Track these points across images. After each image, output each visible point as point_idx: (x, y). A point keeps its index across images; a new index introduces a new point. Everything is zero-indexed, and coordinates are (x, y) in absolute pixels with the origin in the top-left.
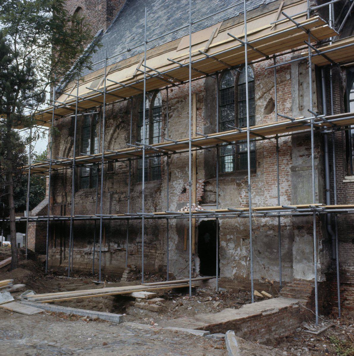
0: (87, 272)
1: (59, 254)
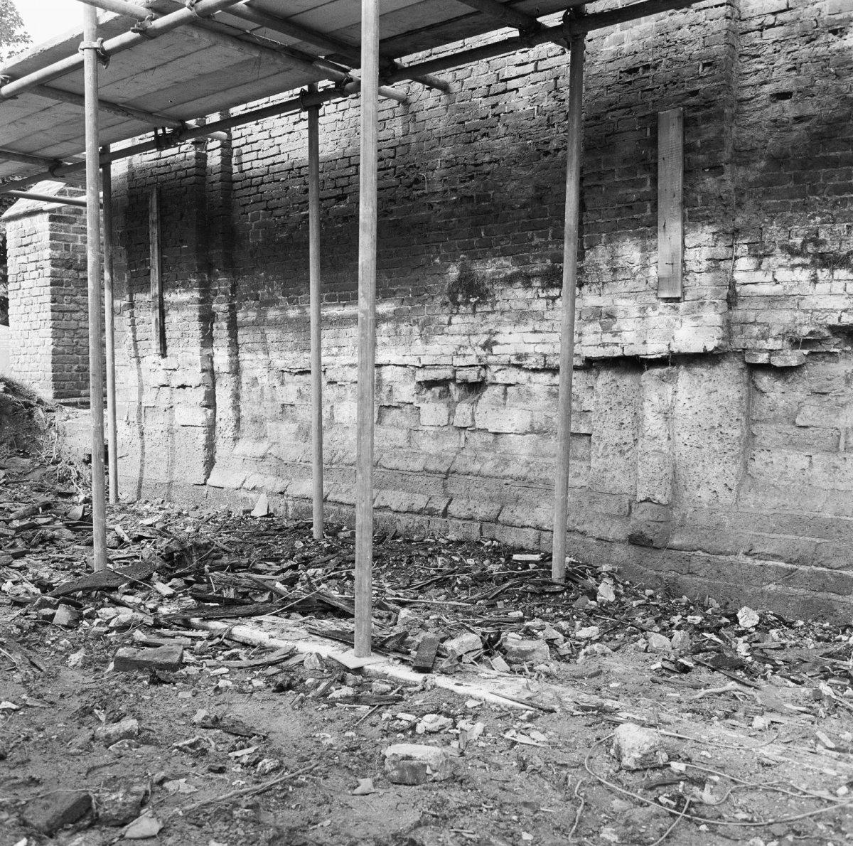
0: (469, 546)
1: (200, 395)
